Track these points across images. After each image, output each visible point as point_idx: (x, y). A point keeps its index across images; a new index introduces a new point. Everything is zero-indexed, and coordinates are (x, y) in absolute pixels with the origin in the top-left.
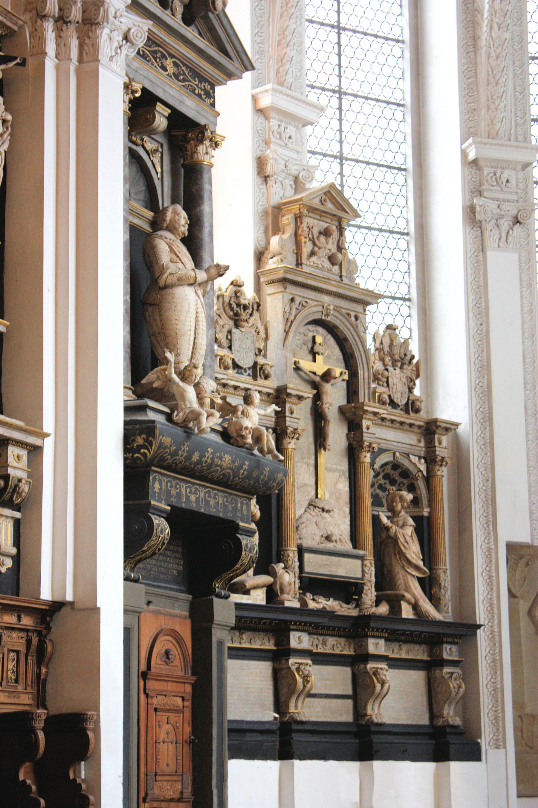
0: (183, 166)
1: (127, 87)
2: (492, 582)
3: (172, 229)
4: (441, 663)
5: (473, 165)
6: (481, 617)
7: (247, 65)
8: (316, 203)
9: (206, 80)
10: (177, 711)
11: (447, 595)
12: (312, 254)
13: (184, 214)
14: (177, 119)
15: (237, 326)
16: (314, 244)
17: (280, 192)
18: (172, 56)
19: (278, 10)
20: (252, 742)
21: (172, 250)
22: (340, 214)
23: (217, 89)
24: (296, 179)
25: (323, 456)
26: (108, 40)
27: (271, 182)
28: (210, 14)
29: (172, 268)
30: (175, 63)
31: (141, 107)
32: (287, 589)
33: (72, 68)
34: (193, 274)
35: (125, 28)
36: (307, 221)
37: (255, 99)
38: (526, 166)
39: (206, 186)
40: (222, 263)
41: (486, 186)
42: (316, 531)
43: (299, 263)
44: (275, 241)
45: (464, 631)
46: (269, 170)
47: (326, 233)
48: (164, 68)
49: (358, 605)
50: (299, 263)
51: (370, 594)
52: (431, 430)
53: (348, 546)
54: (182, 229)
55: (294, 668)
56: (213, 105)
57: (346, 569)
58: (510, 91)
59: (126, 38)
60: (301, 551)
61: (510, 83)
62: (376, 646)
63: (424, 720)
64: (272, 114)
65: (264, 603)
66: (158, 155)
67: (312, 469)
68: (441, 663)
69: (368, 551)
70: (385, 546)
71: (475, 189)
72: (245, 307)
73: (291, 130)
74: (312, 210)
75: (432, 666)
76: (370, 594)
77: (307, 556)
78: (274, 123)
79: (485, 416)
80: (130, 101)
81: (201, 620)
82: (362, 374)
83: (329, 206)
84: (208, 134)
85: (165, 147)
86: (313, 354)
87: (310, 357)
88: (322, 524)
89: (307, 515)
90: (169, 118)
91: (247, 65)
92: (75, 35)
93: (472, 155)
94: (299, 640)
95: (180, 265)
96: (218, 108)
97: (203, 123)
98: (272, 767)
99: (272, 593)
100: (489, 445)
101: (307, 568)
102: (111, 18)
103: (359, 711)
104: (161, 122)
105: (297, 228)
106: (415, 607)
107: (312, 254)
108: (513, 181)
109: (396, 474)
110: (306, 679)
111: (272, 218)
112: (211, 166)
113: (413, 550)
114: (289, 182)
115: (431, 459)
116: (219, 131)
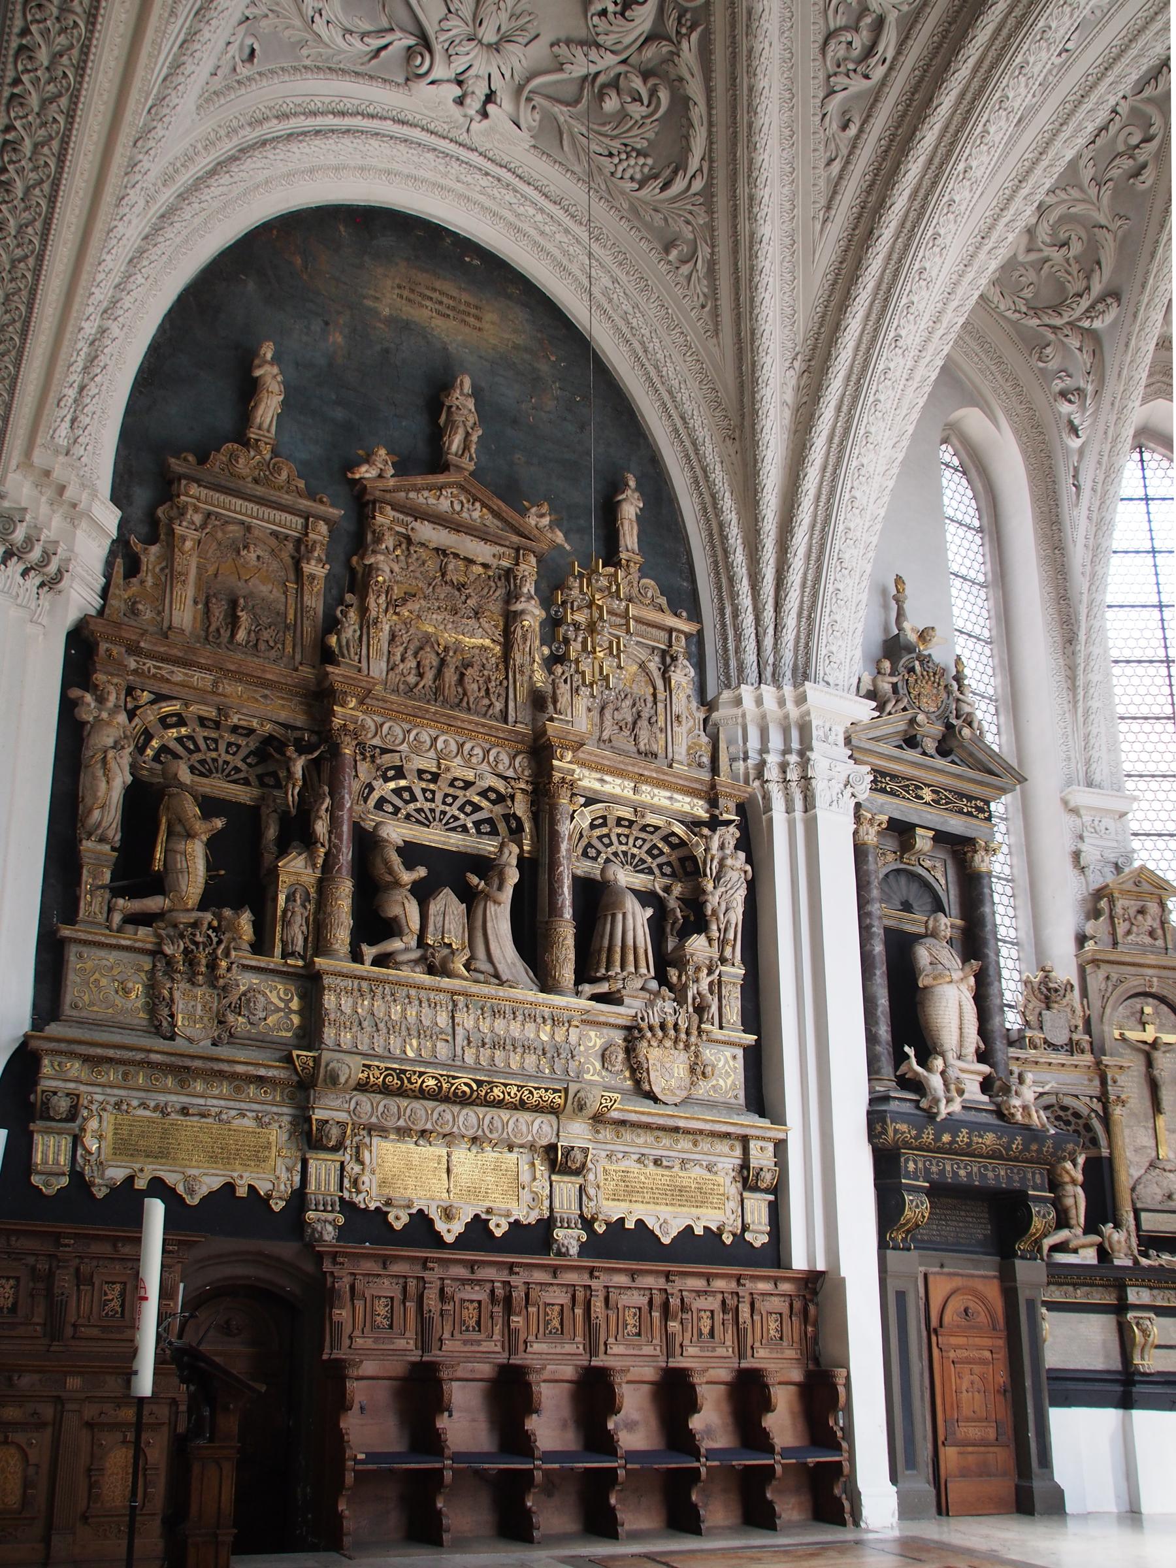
9: (977, 799)
10: (982, 1362)
12: (1129, 932)
15: (1048, 1008)
19: (1081, 720)
20: (1078, 1388)
25: (1161, 1121)
27: (1088, 872)
32: (1116, 1247)
42: (1158, 1191)
43: (1115, 944)
50: (1115, 944)
55: (1133, 1322)
60: (1137, 1213)
65: (1095, 1262)
67: (1151, 1132)
72: (1056, 991)
77: (1144, 1216)
81: (1007, 1280)
85: (949, 862)
87: (1140, 1027)
88: (1165, 1184)
89: (1148, 1177)
98: (1109, 1416)
99: (1104, 1254)
101: (1145, 1226)
107: (1129, 932)
110: (1145, 1333)
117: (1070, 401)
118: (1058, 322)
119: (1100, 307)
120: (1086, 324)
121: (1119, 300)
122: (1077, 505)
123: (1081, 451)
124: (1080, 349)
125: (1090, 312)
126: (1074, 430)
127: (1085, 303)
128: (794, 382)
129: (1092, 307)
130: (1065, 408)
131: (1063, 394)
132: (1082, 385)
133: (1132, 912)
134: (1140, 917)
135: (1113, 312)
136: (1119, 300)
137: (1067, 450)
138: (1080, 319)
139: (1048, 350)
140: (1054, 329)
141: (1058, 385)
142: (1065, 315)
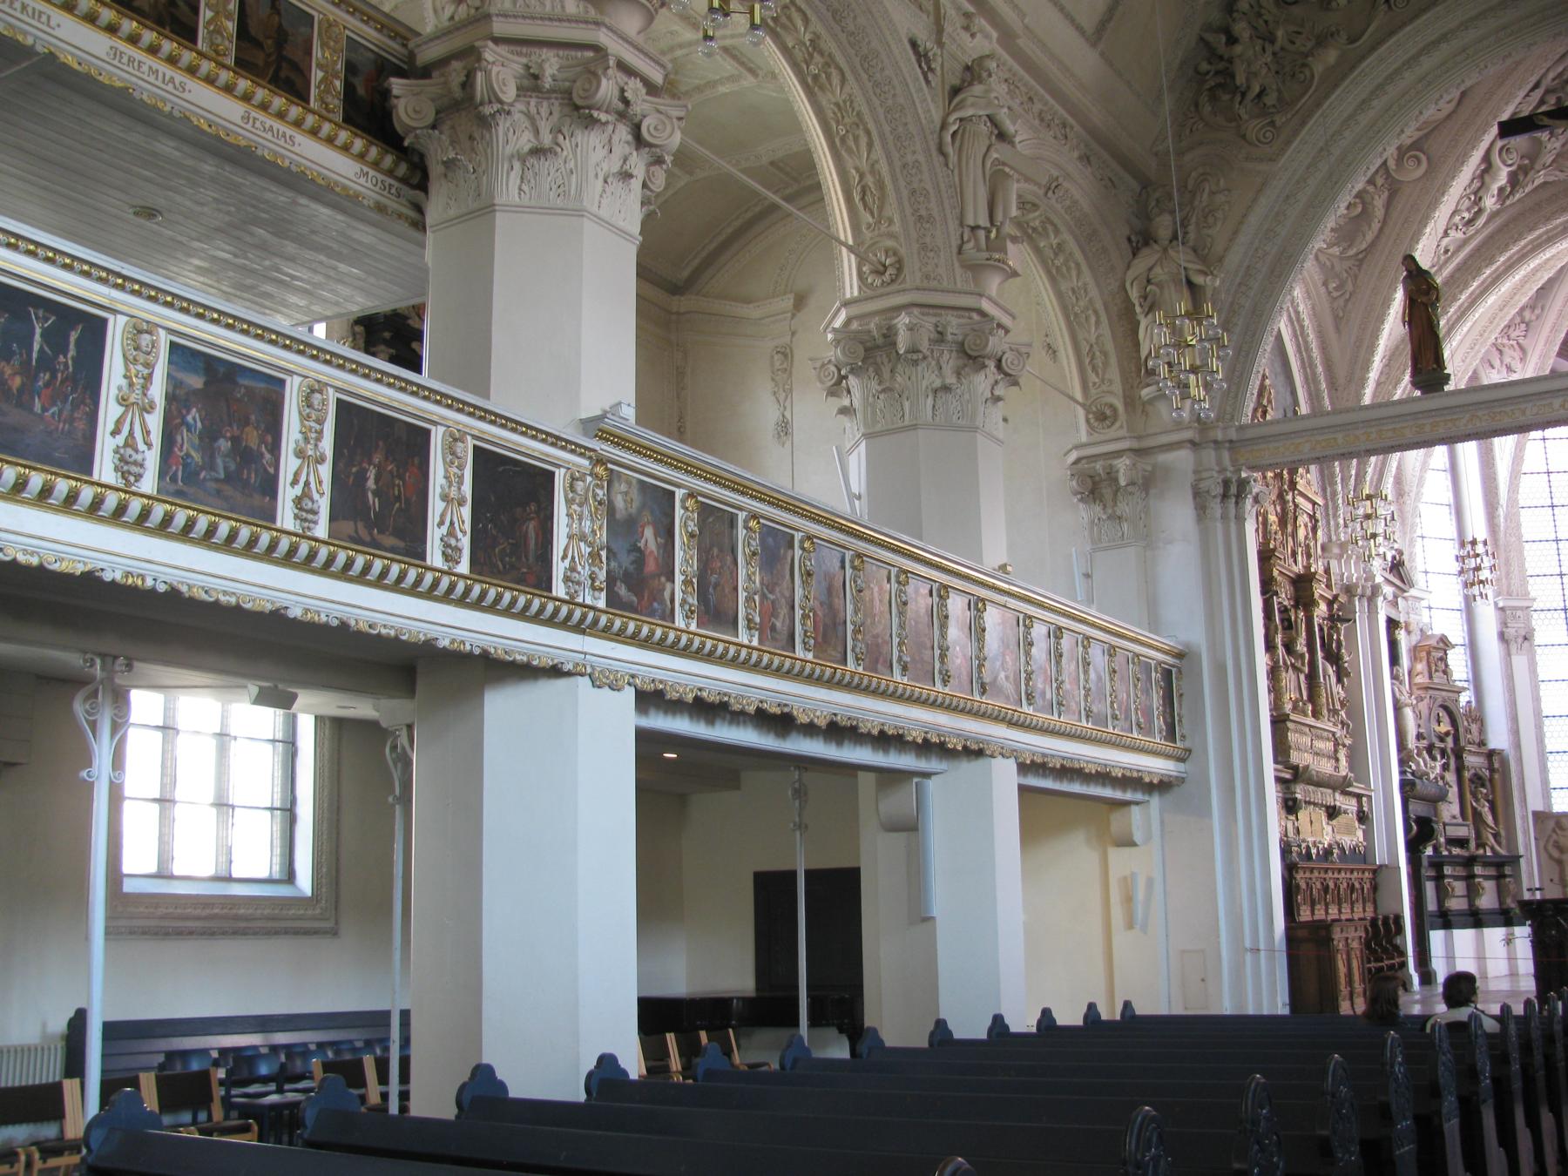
2: (1526, 832)
4: (1505, 876)
6: (1521, 851)
11: (1504, 842)
45: (1514, 860)
49: (1468, 849)
51: (1473, 844)
52: (1491, 754)
53: (1460, 820)
57: (1462, 832)
62: (1478, 870)
63: (1496, 906)
68: (1505, 876)
69: (1470, 822)
70: (1477, 816)
75: (1500, 877)
76: (1473, 844)
79: (1517, 745)
82: (1461, 730)
86: (1439, 722)
94: (1448, 870)
100: (1520, 760)
103: (1471, 904)
106: (1492, 849)
109: (1478, 780)
113: (1489, 819)
115: (1492, 770)
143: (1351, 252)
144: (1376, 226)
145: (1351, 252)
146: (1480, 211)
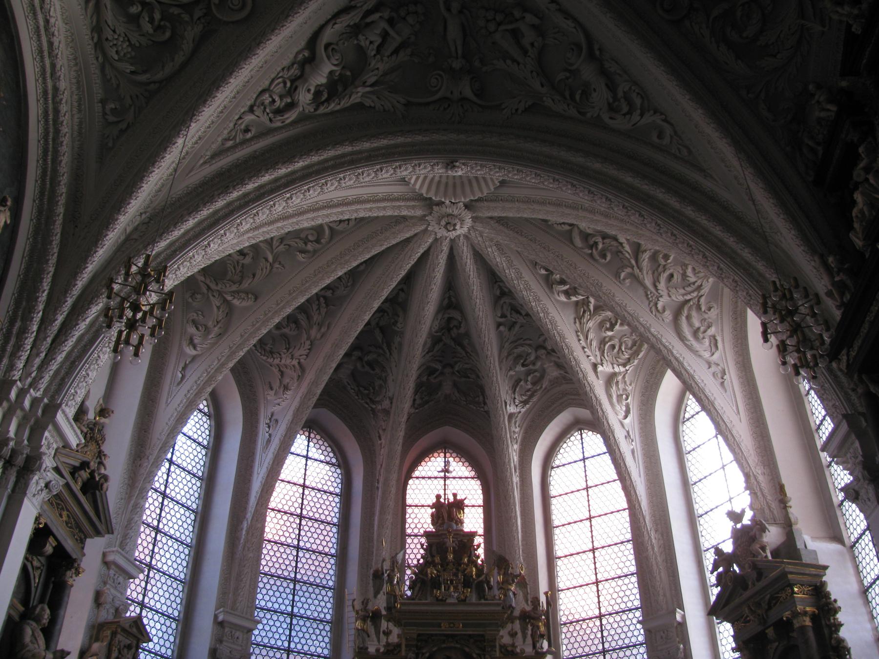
0: (53, 582)
1: (37, 519)
3: (38, 620)
5: (220, 624)
7: (110, 531)
8: (127, 626)
9: (83, 532)
13: (48, 611)
14: (60, 549)
16: (120, 652)
17: (106, 615)
18: (68, 510)
21: (33, 634)
22: (140, 636)
23: (88, 541)
24: (117, 610)
26: (36, 482)
28: (97, 492)
29: (31, 646)
30: (68, 516)
31: (41, 534)
33: (6, 495)
34: (44, 654)
35: (48, 479)
36: (120, 637)
37: (104, 555)
38: (250, 631)
39: (66, 598)
40: (67, 649)
41: (225, 638)
44: (96, 646)
46: (102, 600)
47: (129, 647)
48: (61, 516)
54: (44, 621)
56: (83, 548)
58: (247, 587)
59: (47, 485)
61: (248, 582)
64: (113, 567)
66: (39, 571)
71: (219, 640)
73: (121, 579)
74: (124, 630)
78: (112, 572)
80: (35, 529)
83: (134, 630)
84: (76, 565)
90: (55, 548)
91: (110, 531)
92: (15, 474)
93: (221, 618)
95: (36, 646)
96: (85, 551)
97: (74, 557)
102: (42, 471)
104: (49, 549)
105: (112, 639)
108: (241, 638)
111: (96, 631)
112: (72, 586)
114: (112, 611)
116: (83, 565)
117: (197, 328)
118: (213, 286)
119: (243, 295)
120: (229, 298)
121: (256, 298)
122: (179, 384)
123: (194, 358)
124: (218, 308)
125: (235, 293)
126: (192, 343)
127: (234, 288)
128: (136, 223)
129: (238, 292)
130: (192, 330)
131: (194, 321)
132: (210, 324)
133: (122, 645)
134: (126, 650)
135: (250, 303)
136: (256, 298)
137: (182, 353)
138: (226, 293)
139: (199, 296)
140: (209, 288)
141: (193, 315)
142: (220, 286)
143: (143, 78)
144: (180, 58)
145: (143, 78)
146: (291, 106)
